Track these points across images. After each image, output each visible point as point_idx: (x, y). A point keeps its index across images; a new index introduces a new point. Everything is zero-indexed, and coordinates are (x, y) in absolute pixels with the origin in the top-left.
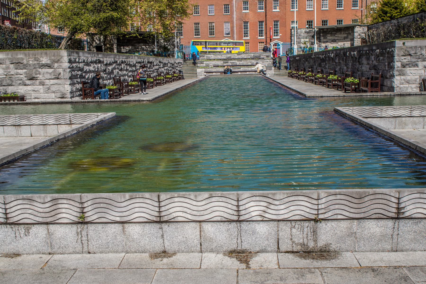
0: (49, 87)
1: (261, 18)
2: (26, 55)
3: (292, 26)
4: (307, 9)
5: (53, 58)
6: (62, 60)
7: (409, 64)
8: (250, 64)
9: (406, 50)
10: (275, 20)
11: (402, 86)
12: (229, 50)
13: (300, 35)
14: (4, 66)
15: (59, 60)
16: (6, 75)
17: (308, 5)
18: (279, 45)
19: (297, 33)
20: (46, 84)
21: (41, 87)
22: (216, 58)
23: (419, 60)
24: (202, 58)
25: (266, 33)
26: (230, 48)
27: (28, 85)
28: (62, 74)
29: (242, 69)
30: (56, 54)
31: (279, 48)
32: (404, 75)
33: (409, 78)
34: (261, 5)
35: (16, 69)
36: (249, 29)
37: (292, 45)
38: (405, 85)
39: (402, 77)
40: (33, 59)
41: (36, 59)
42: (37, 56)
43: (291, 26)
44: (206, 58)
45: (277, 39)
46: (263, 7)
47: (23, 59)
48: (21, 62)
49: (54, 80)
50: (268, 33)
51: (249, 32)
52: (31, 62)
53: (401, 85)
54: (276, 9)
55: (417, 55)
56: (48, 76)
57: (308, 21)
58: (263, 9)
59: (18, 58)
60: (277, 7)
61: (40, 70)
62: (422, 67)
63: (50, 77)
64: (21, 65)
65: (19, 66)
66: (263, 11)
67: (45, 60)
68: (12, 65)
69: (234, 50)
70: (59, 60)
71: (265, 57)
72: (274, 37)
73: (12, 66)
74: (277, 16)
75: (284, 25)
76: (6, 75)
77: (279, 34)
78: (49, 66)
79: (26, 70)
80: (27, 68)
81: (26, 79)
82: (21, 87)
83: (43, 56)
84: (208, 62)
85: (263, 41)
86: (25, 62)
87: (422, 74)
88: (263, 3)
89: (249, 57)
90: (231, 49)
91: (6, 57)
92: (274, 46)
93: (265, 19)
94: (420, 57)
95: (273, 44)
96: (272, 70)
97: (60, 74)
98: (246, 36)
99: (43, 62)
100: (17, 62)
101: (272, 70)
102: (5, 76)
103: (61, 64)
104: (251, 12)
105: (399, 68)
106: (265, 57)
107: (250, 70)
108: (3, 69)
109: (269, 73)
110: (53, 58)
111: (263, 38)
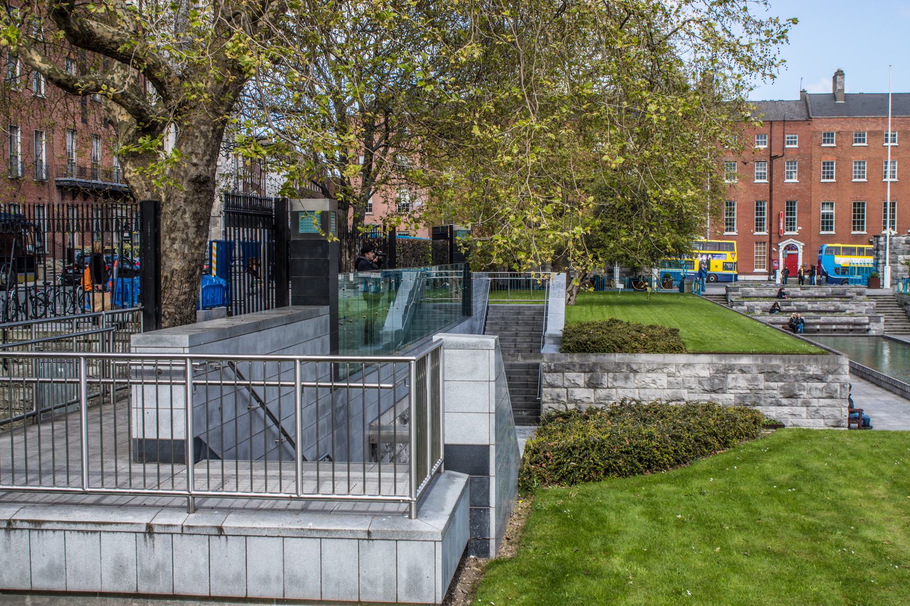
0: (818, 410)
1: (761, 196)
2: (784, 361)
3: (823, 211)
4: (854, 180)
5: (826, 367)
6: (840, 370)
8: (832, 308)
10: (789, 198)
12: (704, 258)
13: (895, 248)
14: (749, 376)
15: (836, 370)
16: (750, 390)
17: (855, 172)
18: (797, 249)
19: (891, 244)
20: (812, 405)
21: (804, 409)
22: (761, 293)
24: (733, 293)
25: (771, 225)
26: (707, 255)
27: (785, 405)
28: (839, 392)
29: (823, 319)
30: (832, 361)
31: (797, 254)
34: (761, 169)
35: (767, 381)
36: (735, 217)
37: (881, 265)
40: (795, 368)
41: (800, 368)
42: (801, 364)
43: (822, 211)
44: (740, 293)
45: (793, 237)
46: (765, 174)
47: (780, 367)
48: (777, 371)
49: (826, 400)
50: (774, 225)
51: (735, 222)
52: (791, 372)
54: (791, 178)
56: (818, 394)
57: (855, 204)
58: (765, 178)
59: (772, 366)
60: (794, 174)
61: (805, 384)
63: (820, 395)
64: (775, 376)
65: (772, 376)
66: (765, 181)
67: (813, 370)
68: (762, 375)
69: (715, 259)
70: (836, 370)
71: (854, 294)
72: (787, 233)
73: (761, 377)
74: (794, 192)
75: (807, 209)
76: (750, 390)
77: (796, 226)
78: (819, 379)
79: (783, 383)
80: (785, 380)
81: (781, 396)
82: (772, 408)
83: (811, 363)
84: (751, 303)
85: (764, 240)
86: (782, 371)
88: (765, 165)
89: (824, 294)
90: (710, 256)
91: (754, 363)
92: (785, 248)
93: (768, 197)
95: (785, 245)
96: (880, 322)
97: (836, 391)
98: (730, 229)
99: (811, 373)
100: (770, 371)
101: (880, 322)
102: (749, 391)
103: (838, 377)
104: (741, 183)
106: (854, 294)
107: (838, 321)
108: (747, 380)
109: (875, 328)
110: (826, 367)
111: (765, 233)
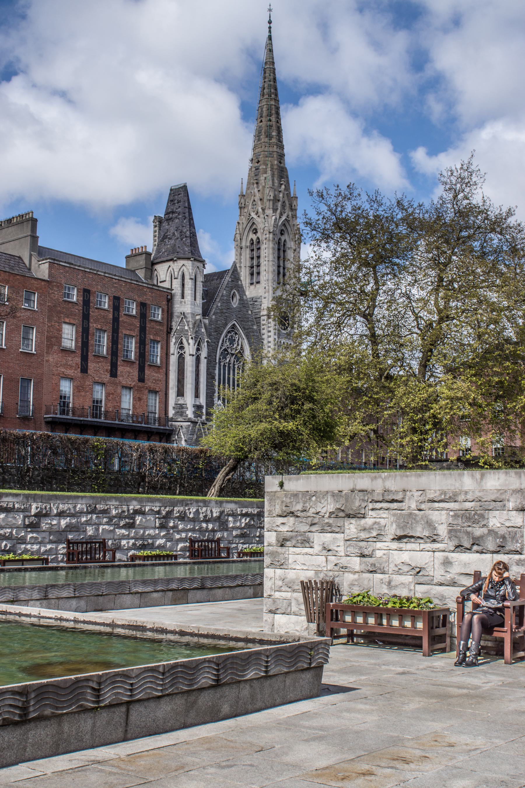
7: (292, 537)
9: (282, 502)
11: (277, 595)
23: (314, 529)
32: (281, 566)
33: (291, 575)
38: (284, 594)
39: (279, 572)
53: (277, 593)
55: (309, 514)
62: (320, 548)
87: (319, 566)
94: (316, 521)
105: (271, 548)
